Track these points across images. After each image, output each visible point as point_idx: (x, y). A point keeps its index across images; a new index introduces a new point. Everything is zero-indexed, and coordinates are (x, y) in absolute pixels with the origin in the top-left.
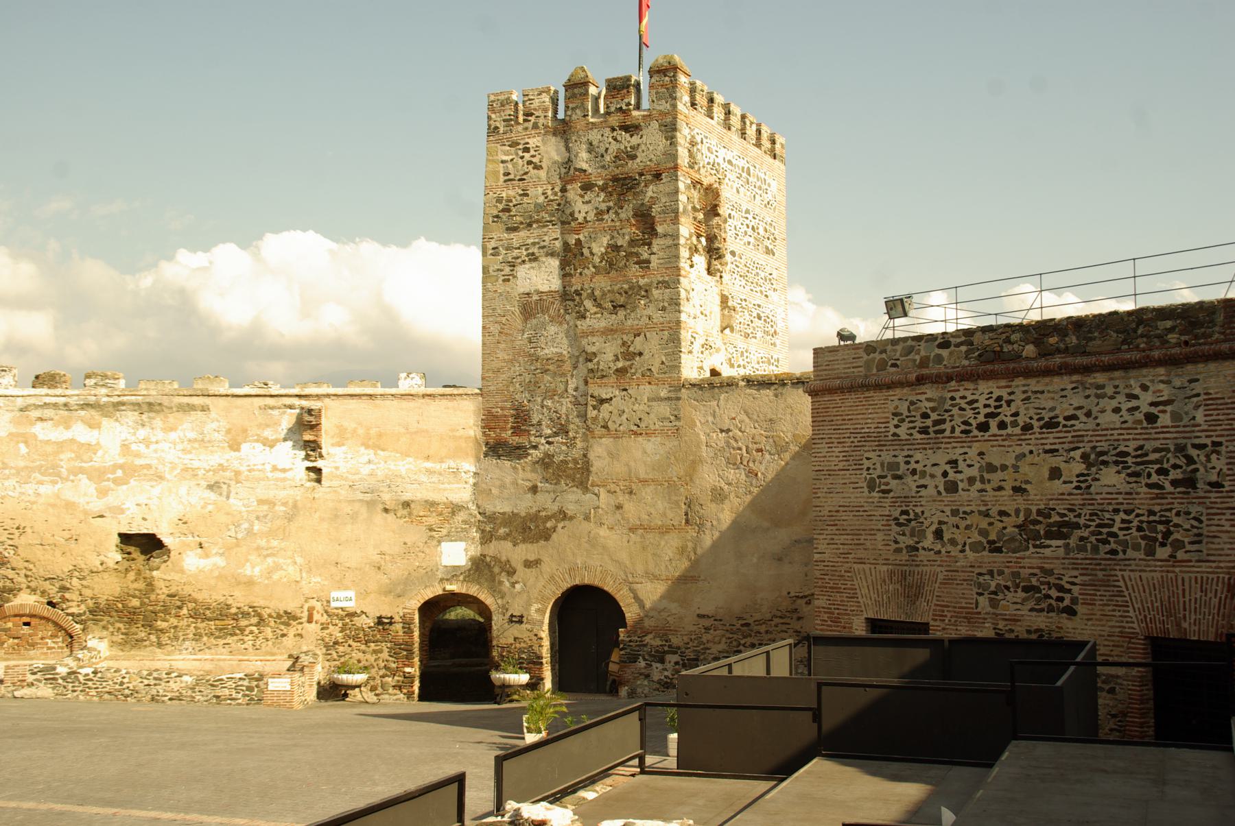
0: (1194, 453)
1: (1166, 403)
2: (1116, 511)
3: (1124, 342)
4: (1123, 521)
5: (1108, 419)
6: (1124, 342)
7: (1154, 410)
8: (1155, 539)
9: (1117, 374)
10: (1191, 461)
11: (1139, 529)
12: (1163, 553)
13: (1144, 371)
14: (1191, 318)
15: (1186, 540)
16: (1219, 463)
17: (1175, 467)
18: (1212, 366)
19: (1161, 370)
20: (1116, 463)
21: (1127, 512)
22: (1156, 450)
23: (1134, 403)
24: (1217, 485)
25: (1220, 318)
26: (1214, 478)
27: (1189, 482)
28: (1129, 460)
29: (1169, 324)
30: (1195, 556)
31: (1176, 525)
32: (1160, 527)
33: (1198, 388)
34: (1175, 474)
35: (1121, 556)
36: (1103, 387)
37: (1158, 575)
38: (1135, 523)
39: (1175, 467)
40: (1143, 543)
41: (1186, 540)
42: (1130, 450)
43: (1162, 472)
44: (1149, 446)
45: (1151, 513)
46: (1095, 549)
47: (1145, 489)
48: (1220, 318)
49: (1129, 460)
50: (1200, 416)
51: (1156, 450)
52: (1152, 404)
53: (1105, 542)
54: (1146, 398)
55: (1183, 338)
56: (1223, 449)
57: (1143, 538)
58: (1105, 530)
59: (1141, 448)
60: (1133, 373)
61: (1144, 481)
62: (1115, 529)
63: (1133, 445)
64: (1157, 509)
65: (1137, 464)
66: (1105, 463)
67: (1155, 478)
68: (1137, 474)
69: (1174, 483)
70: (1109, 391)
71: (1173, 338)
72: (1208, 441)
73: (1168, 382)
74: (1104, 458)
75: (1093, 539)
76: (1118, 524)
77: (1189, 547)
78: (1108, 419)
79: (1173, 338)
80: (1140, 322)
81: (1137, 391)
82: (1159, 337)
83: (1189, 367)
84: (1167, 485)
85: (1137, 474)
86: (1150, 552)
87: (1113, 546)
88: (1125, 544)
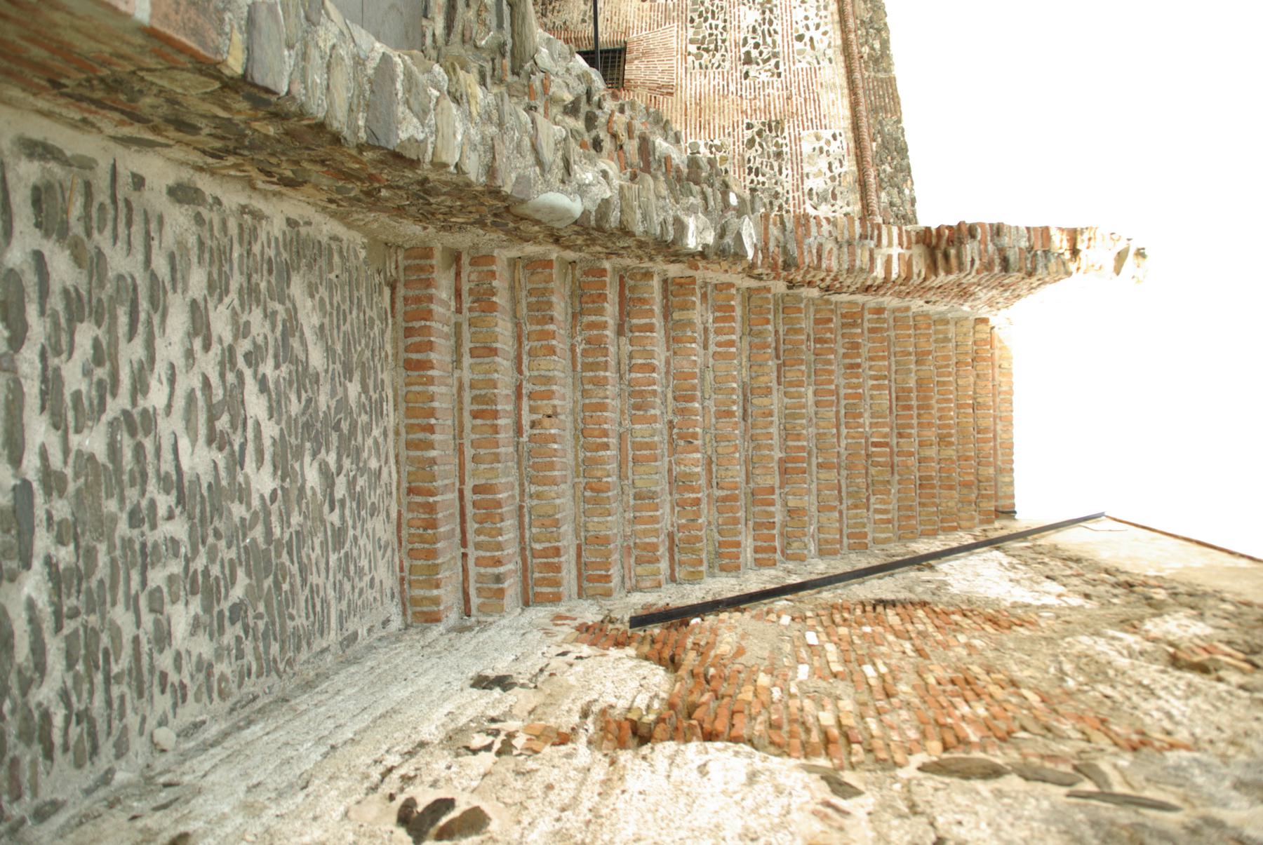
0: (773, 62)
1: (813, 47)
2: (725, 21)
3: (863, 22)
4: (717, 27)
5: (799, 14)
6: (863, 22)
7: (807, 39)
8: (703, 43)
9: (836, 17)
10: (765, 61)
11: (711, 35)
12: (693, 48)
13: (839, 33)
14: (881, 59)
15: (702, 61)
16: (764, 77)
17: (761, 53)
18: (843, 71)
19: (839, 42)
20: (764, 19)
21: (724, 28)
22: (774, 42)
23: (812, 28)
24: (747, 75)
25: (881, 75)
26: (751, 74)
27: (748, 60)
28: (766, 26)
29: (877, 46)
30: (690, 65)
31: (714, 56)
32: (712, 46)
33: (825, 63)
34: (755, 53)
35: (689, 25)
36: (826, 8)
37: (675, 45)
38: (715, 32)
39: (761, 53)
40: (700, 37)
41: (702, 61)
42: (774, 26)
43: (757, 46)
44: (778, 38)
45: (724, 41)
46: (694, 11)
47: (742, 37)
48: (881, 75)
49: (766, 26)
50: (804, 65)
51: (774, 42)
52: (811, 39)
53: (700, 16)
54: (817, 35)
55: (866, 56)
56: (775, 78)
57: (704, 37)
58: (709, 15)
59: (776, 32)
60: (837, 27)
61: (750, 36)
62: (710, 21)
63: (779, 29)
64: (727, 44)
65: (763, 32)
66: (764, 13)
67: (751, 42)
68: (754, 30)
69: (748, 53)
70: (823, 13)
71: (866, 50)
72: (781, 69)
73: (829, 46)
74: (768, 12)
75: (702, 9)
76: (714, 23)
77: (697, 63)
78: (799, 14)
79: (866, 50)
80: (879, 31)
81: (822, 29)
82: (866, 42)
83: (842, 58)
84: (746, 49)
85: (754, 30)
86: (692, 42)
87: (697, 20)
88: (699, 27)
